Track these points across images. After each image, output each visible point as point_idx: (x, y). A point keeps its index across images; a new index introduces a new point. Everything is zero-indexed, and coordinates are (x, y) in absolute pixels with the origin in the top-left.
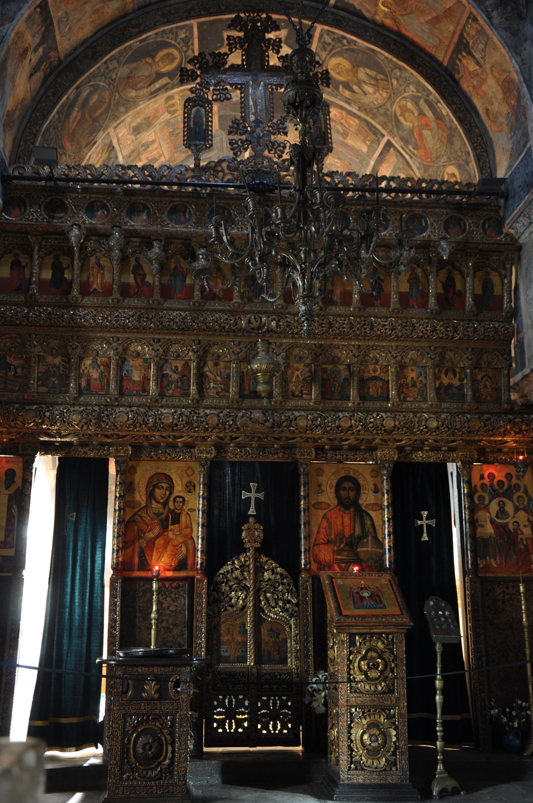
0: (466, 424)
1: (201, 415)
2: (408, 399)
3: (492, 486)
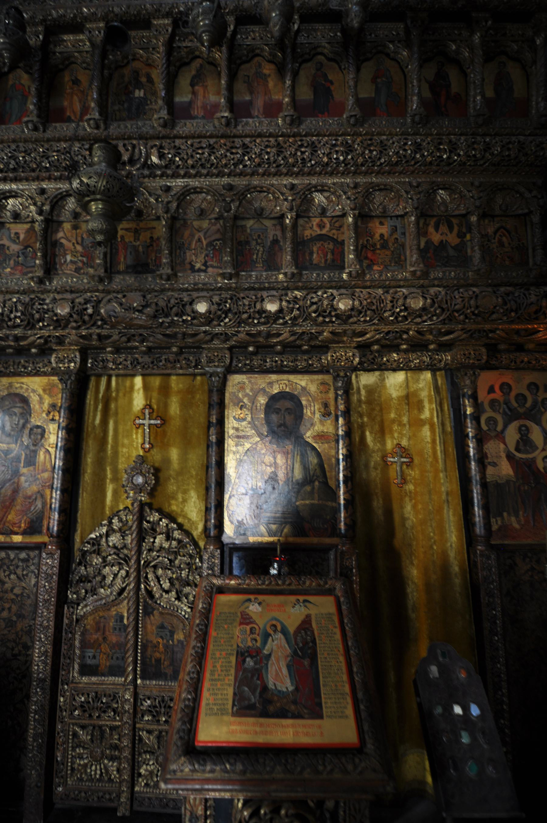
0: (472, 302)
1: (47, 301)
2: (376, 268)
3: (507, 403)
